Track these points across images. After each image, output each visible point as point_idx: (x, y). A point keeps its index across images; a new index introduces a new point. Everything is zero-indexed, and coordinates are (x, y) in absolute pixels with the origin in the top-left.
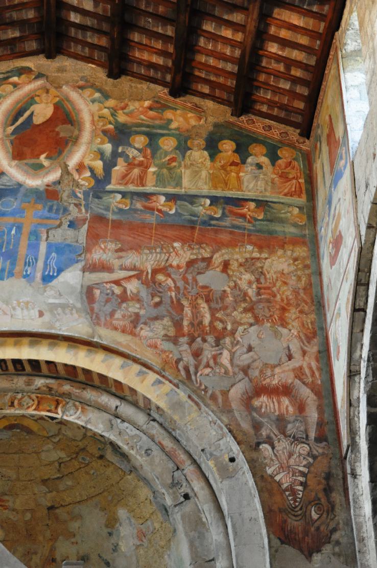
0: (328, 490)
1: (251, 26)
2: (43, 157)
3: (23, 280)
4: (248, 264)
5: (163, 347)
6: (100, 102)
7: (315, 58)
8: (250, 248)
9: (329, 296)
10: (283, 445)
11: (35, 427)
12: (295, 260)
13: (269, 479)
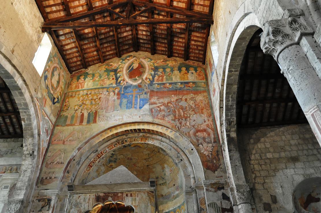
0: (218, 155)
1: (186, 38)
2: (137, 77)
4: (192, 99)
5: (171, 122)
6: (150, 61)
7: (204, 44)
8: (192, 94)
9: (214, 105)
10: (205, 145)
11: (141, 146)
12: (204, 96)
13: (202, 153)
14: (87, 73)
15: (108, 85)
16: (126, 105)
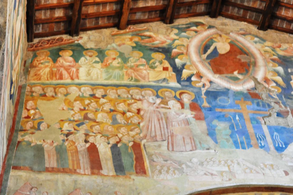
3: (260, 149)
14: (79, 45)
15: (155, 82)
16: (231, 136)
